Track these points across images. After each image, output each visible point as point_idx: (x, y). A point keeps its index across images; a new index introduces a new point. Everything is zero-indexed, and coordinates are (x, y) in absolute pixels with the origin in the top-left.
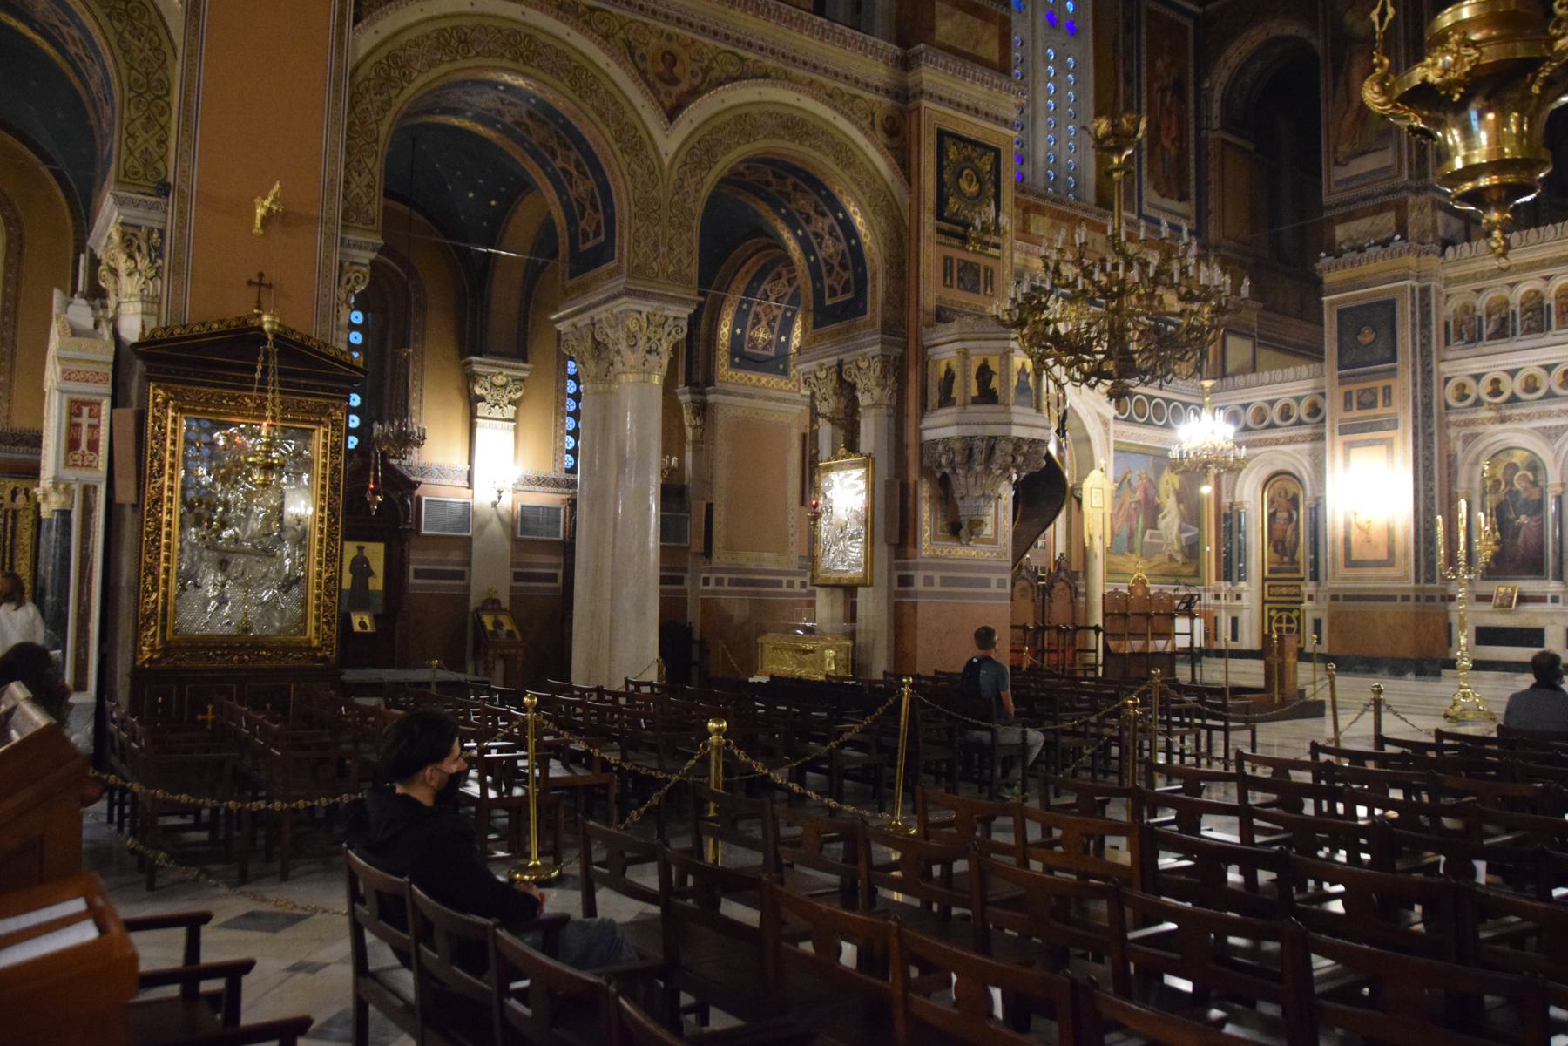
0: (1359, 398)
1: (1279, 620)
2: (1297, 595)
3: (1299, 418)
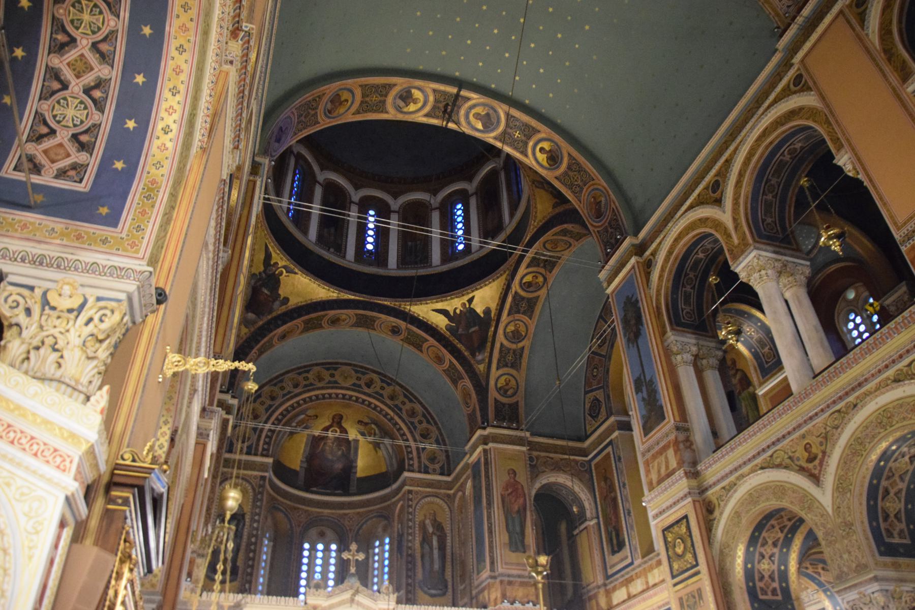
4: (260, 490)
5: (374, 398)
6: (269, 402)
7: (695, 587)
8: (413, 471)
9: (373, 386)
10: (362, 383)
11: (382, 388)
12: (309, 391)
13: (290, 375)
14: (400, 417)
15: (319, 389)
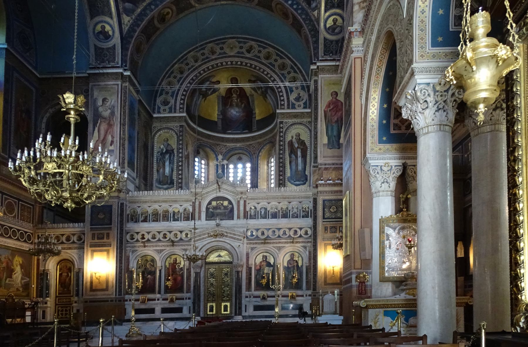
0: (97, 236)
1: (62, 311)
2: (69, 302)
3: (74, 241)
4: (181, 134)
5: (254, 60)
6: (179, 76)
8: (284, 109)
9: (253, 51)
10: (244, 50)
11: (260, 52)
12: (205, 63)
13: (192, 53)
14: (274, 71)
15: (212, 60)
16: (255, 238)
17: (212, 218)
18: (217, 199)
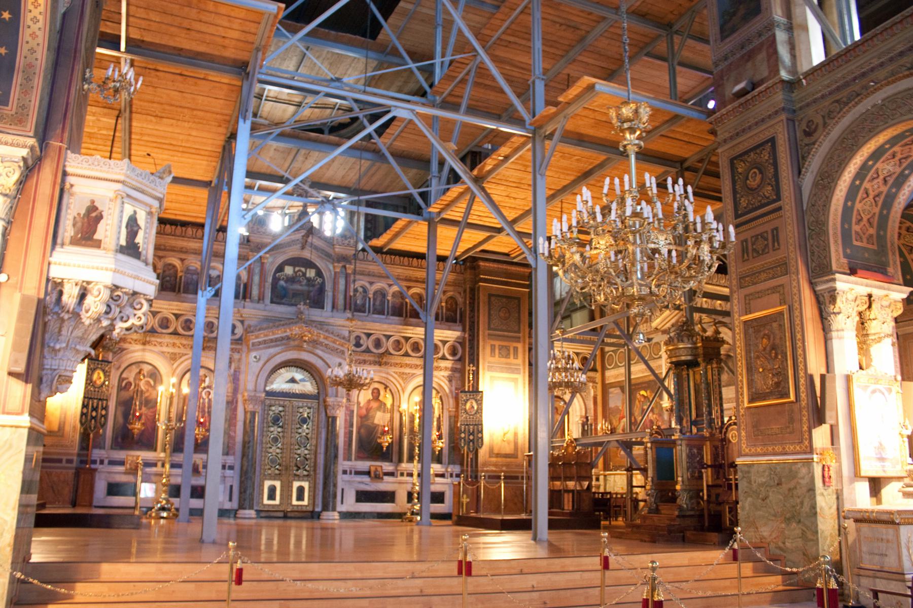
7: (768, 228)
16: (364, 352)
17: (283, 301)
18: (293, 262)
